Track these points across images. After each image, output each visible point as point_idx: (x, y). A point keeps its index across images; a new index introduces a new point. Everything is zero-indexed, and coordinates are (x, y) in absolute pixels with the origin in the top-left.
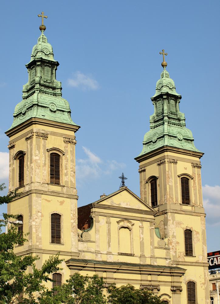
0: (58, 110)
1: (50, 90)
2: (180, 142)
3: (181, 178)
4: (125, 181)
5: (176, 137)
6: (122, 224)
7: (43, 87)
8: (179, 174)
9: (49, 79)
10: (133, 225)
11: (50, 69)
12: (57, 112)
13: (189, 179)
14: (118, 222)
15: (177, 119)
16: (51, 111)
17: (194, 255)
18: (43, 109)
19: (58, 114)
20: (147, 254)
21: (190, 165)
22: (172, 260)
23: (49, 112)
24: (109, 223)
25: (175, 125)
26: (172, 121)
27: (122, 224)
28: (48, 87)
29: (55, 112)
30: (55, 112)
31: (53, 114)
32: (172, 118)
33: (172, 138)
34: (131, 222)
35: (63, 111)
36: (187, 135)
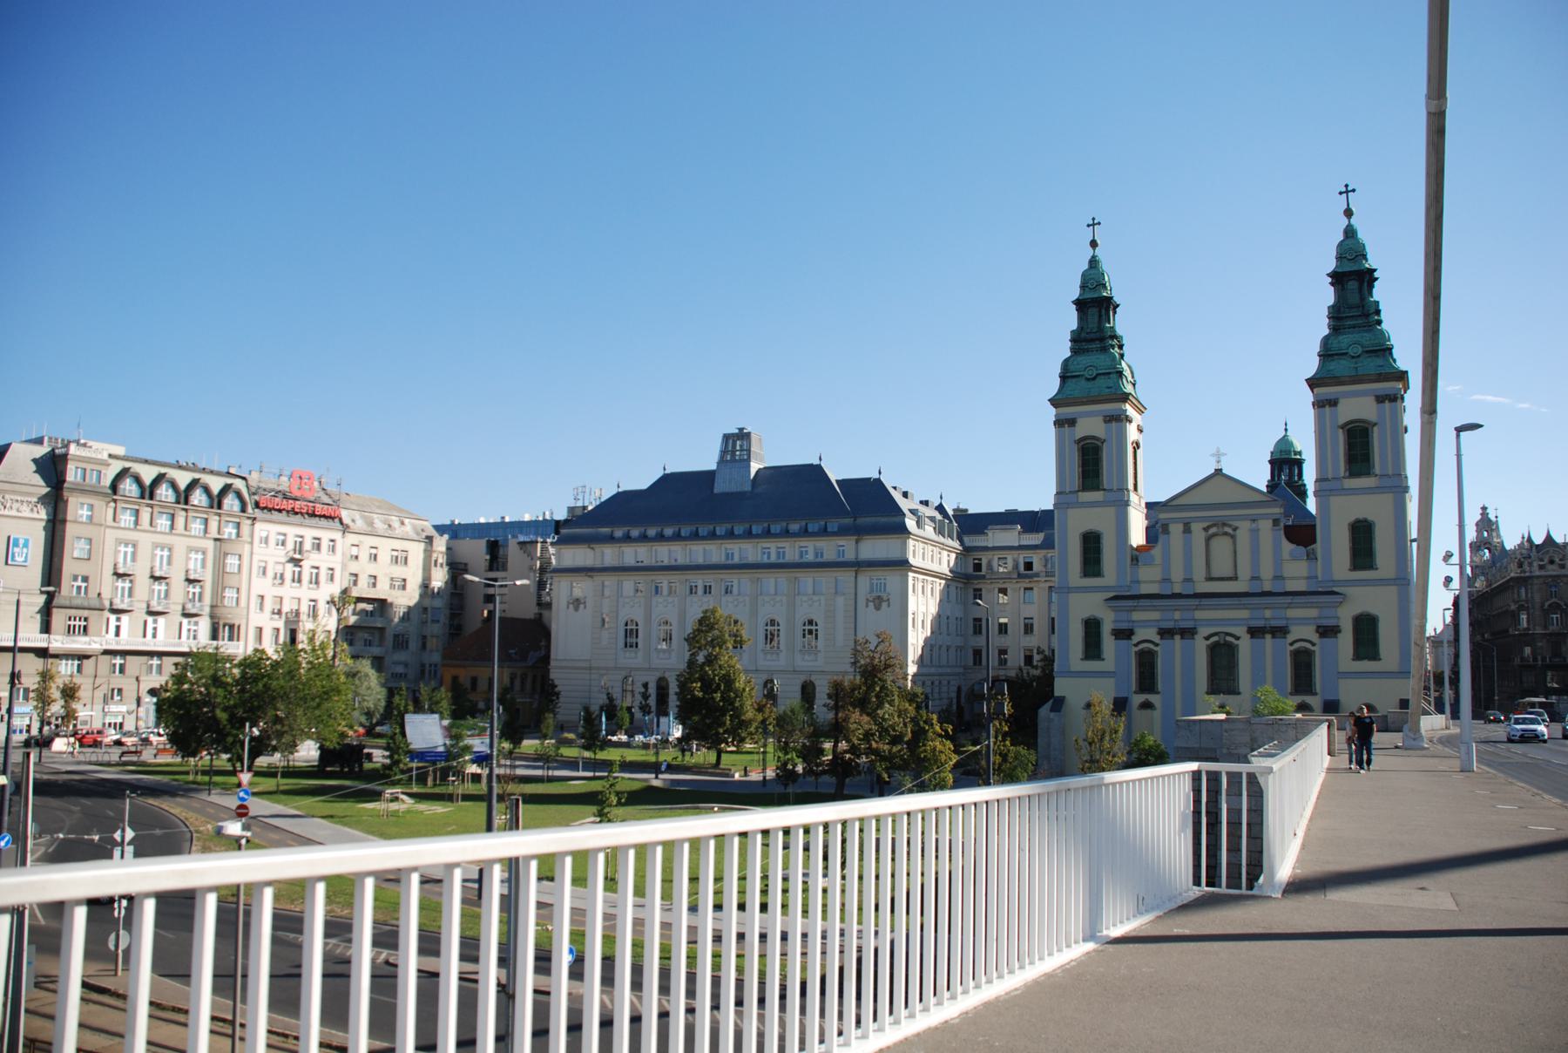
0: (1100, 374)
1: (1097, 345)
2: (1354, 360)
3: (1348, 430)
4: (1222, 458)
5: (1346, 354)
6: (1214, 530)
7: (1084, 344)
8: (1342, 421)
9: (1096, 325)
10: (1235, 529)
11: (1097, 309)
12: (1099, 377)
13: (1367, 429)
14: (1206, 529)
15: (1360, 316)
16: (1088, 379)
17: (1375, 567)
18: (1074, 380)
19: (1101, 382)
20: (1267, 572)
21: (1370, 402)
22: (1320, 579)
23: (1083, 382)
24: (1187, 530)
25: (1354, 328)
26: (1348, 323)
27: (1214, 530)
28: (1092, 340)
29: (1094, 379)
30: (1094, 379)
31: (1090, 384)
32: (1346, 317)
33: (1336, 357)
34: (1230, 526)
35: (1109, 373)
36: (1376, 342)
